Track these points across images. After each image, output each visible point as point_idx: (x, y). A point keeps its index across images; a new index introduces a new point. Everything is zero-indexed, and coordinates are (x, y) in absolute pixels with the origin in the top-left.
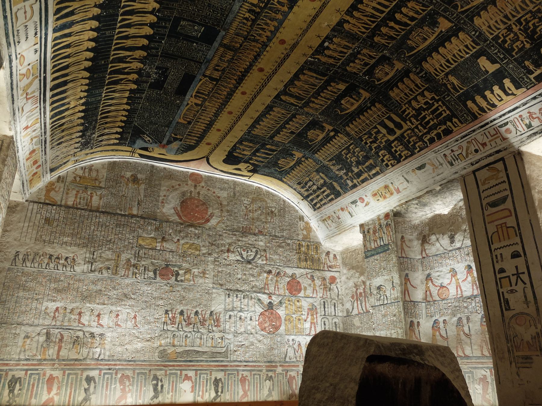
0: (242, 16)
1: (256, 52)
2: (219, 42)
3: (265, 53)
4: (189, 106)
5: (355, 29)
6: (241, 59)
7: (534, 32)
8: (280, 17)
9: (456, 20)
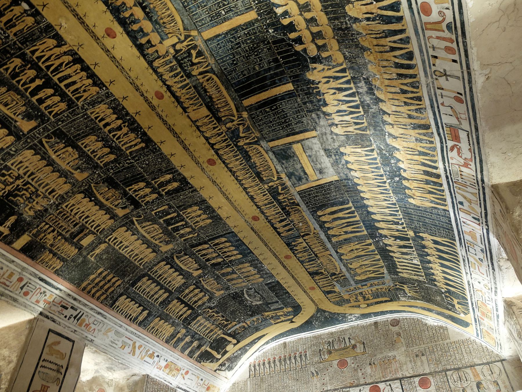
5: (42, 47)
7: (16, 196)
9: (32, 136)
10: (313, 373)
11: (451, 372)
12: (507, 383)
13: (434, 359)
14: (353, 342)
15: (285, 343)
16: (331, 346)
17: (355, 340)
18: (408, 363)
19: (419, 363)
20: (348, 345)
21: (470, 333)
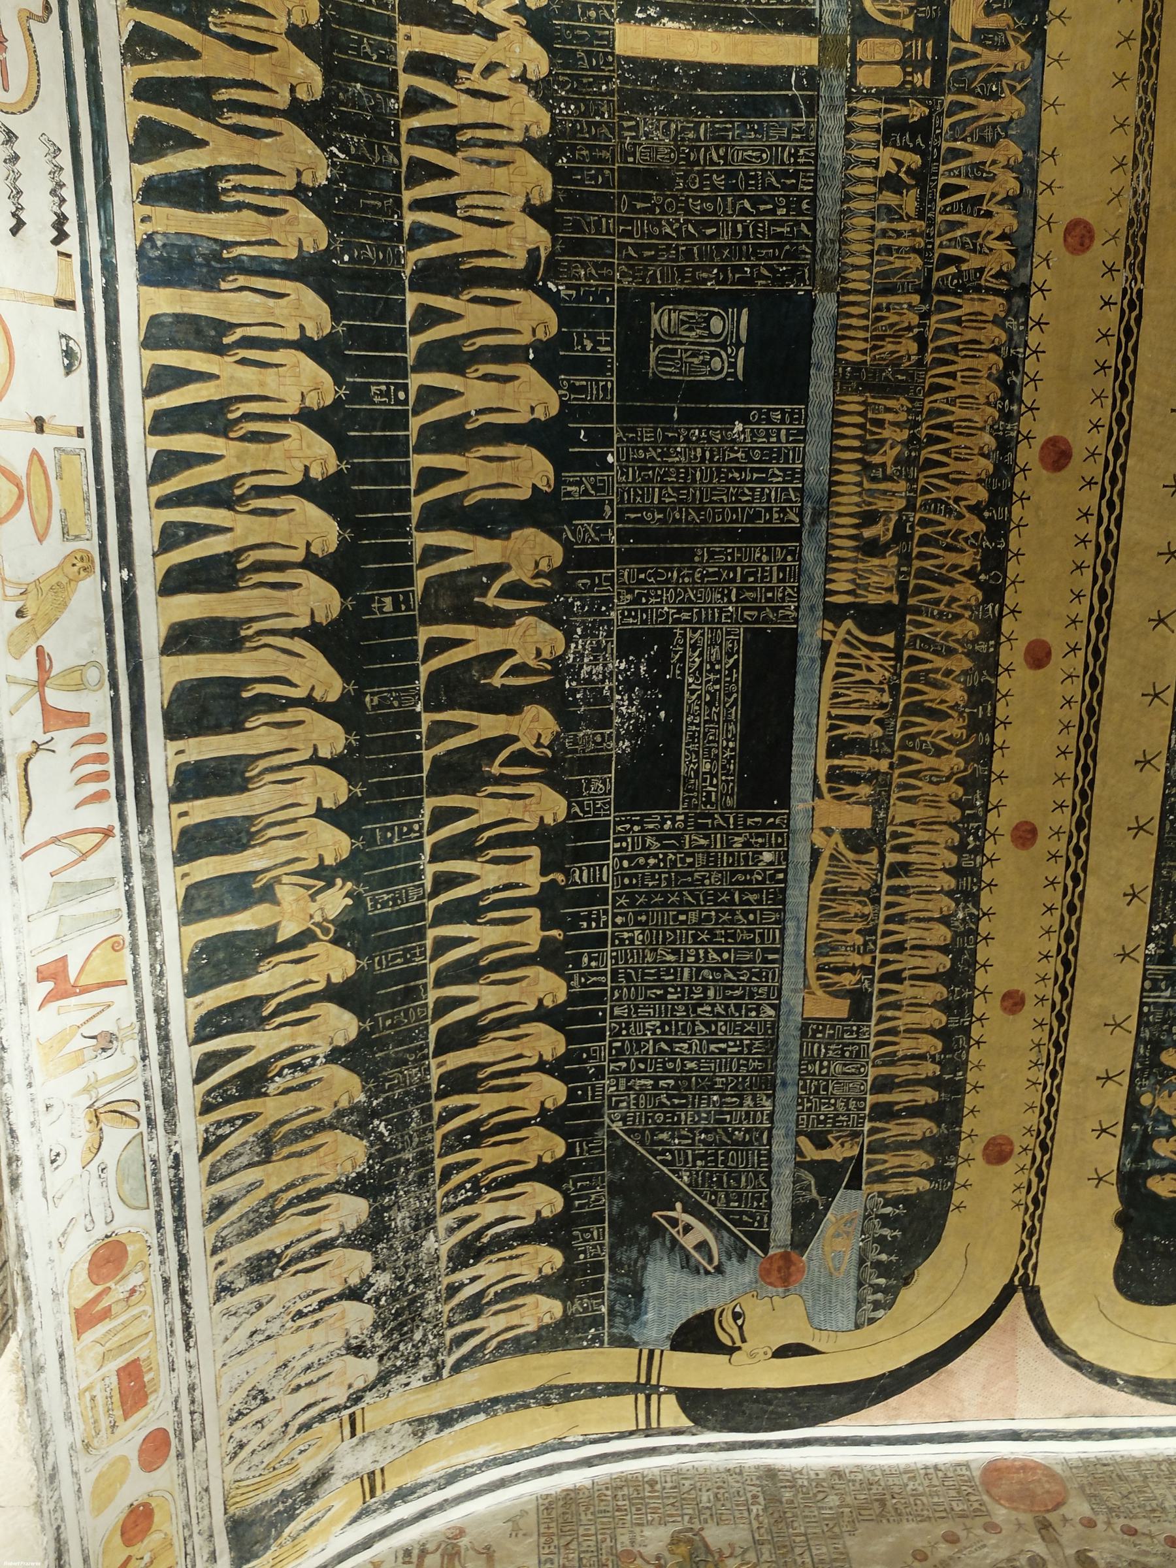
0: (868, 172)
1: (995, 350)
2: (828, 364)
3: (1033, 338)
4: (824, 864)
6: (948, 427)
8: (1012, 107)
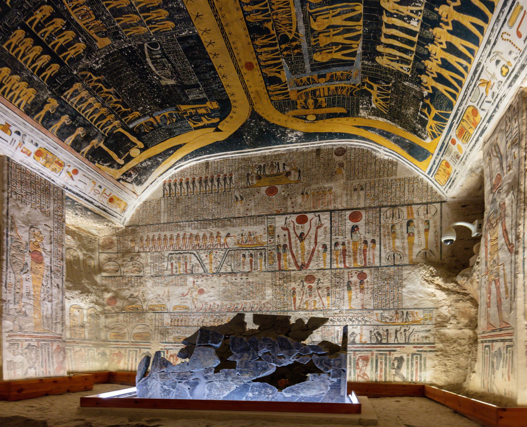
10: (237, 198)
11: (385, 209)
12: (438, 224)
13: (373, 194)
14: (287, 169)
15: (207, 163)
16: (262, 171)
17: (291, 166)
18: (344, 196)
19: (355, 197)
20: (281, 171)
21: (420, 170)
